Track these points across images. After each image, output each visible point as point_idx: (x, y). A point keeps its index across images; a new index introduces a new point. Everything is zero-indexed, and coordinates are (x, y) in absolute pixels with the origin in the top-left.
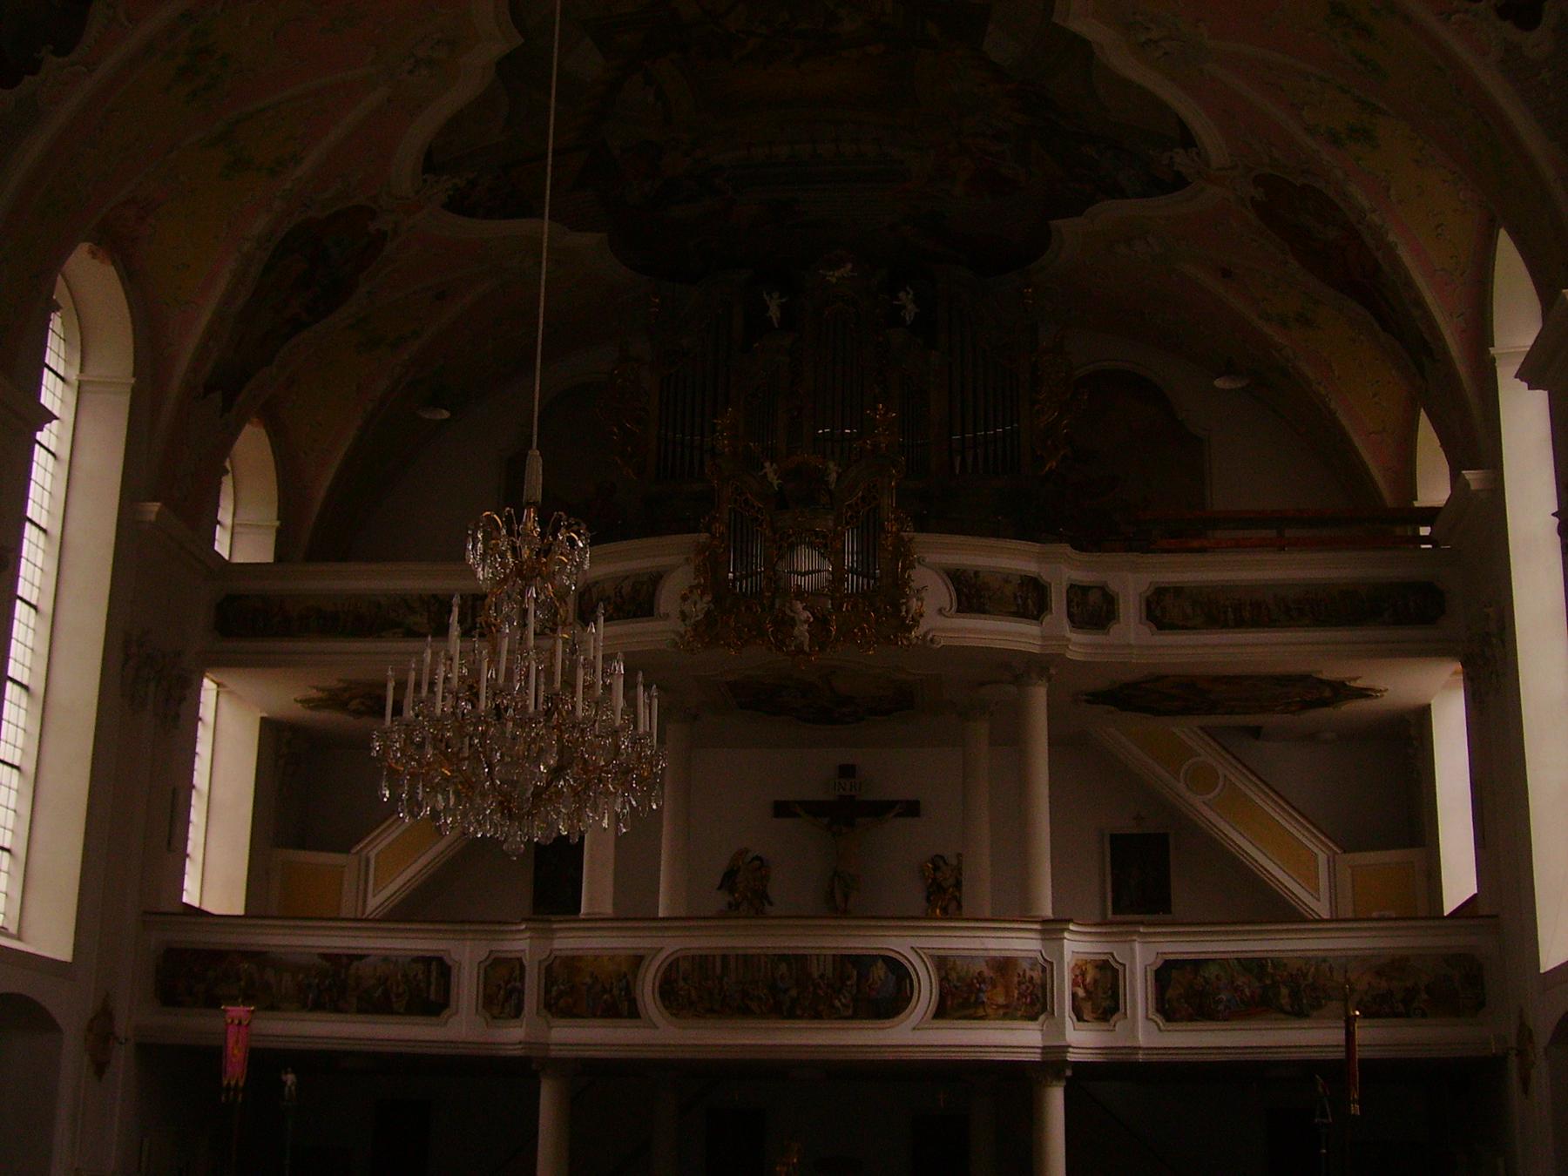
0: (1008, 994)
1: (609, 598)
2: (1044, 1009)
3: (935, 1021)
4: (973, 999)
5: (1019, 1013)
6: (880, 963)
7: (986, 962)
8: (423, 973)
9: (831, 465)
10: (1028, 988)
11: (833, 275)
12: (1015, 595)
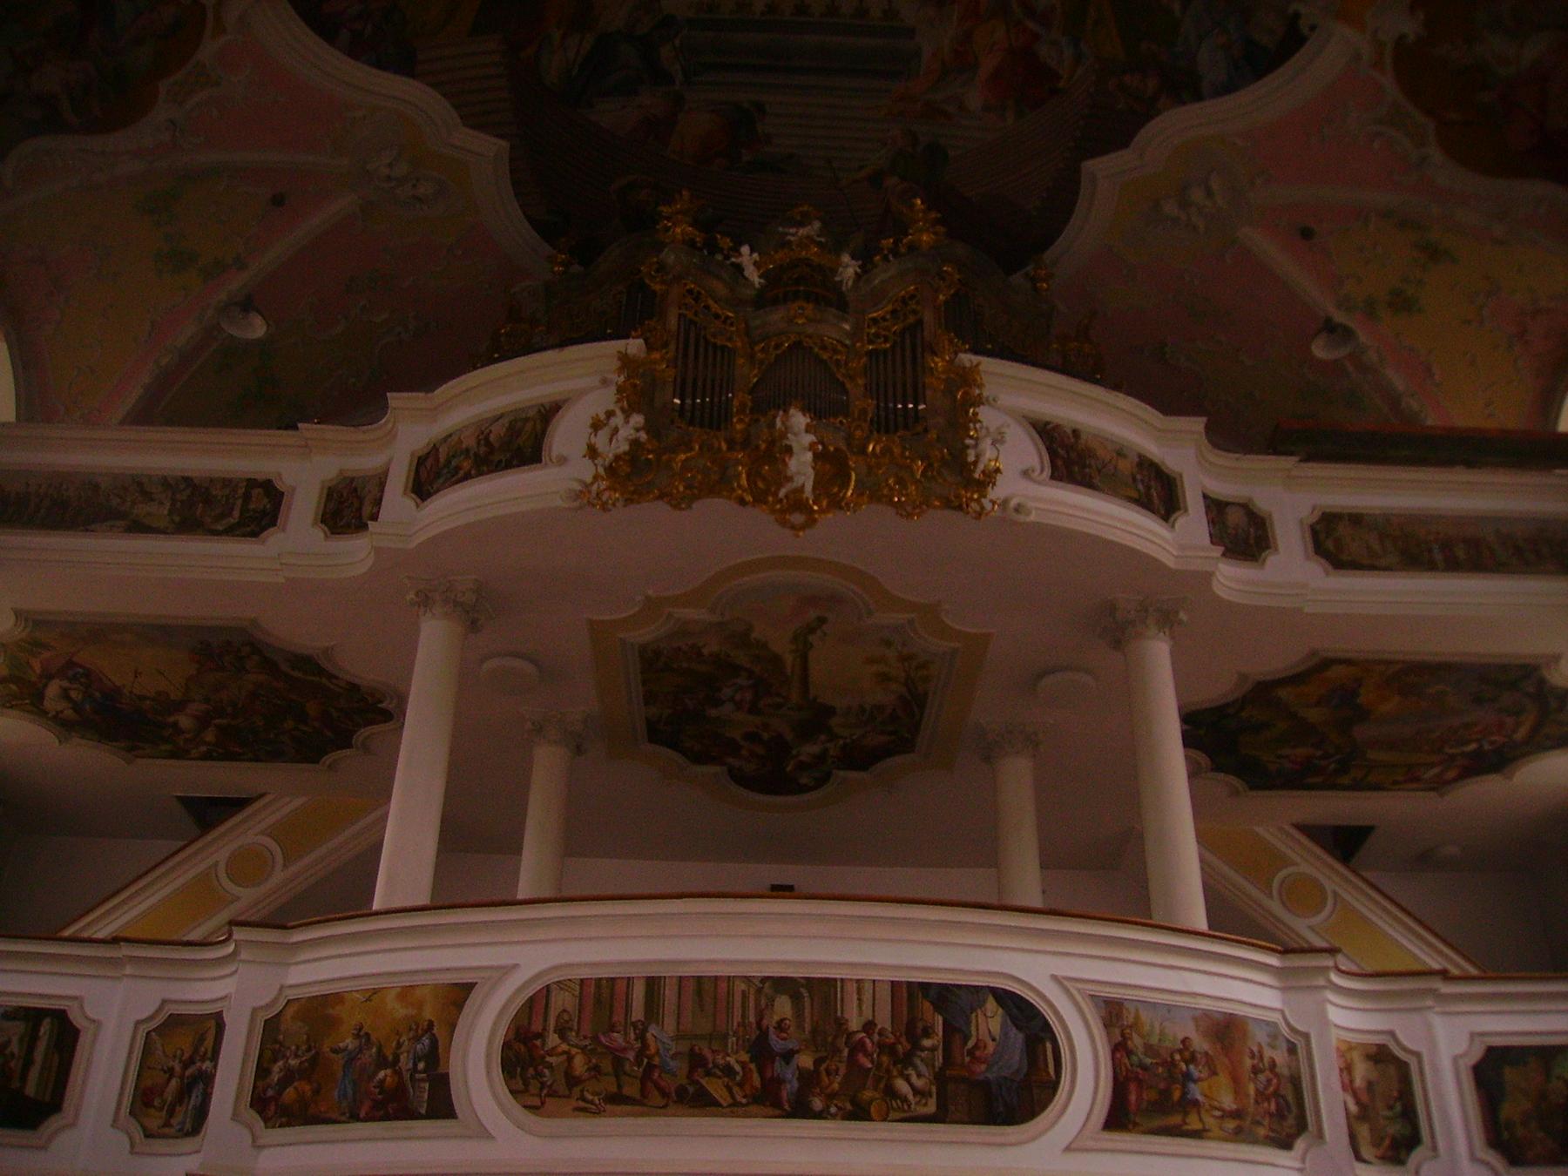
0: (1238, 1090)
1: (467, 450)
2: (1302, 1127)
3: (1107, 1135)
4: (1177, 1095)
5: (1262, 1132)
6: (991, 1004)
7: (1195, 1019)
8: (21, 1040)
9: (846, 258)
10: (1269, 1081)
11: (797, 232)
12: (1134, 479)
